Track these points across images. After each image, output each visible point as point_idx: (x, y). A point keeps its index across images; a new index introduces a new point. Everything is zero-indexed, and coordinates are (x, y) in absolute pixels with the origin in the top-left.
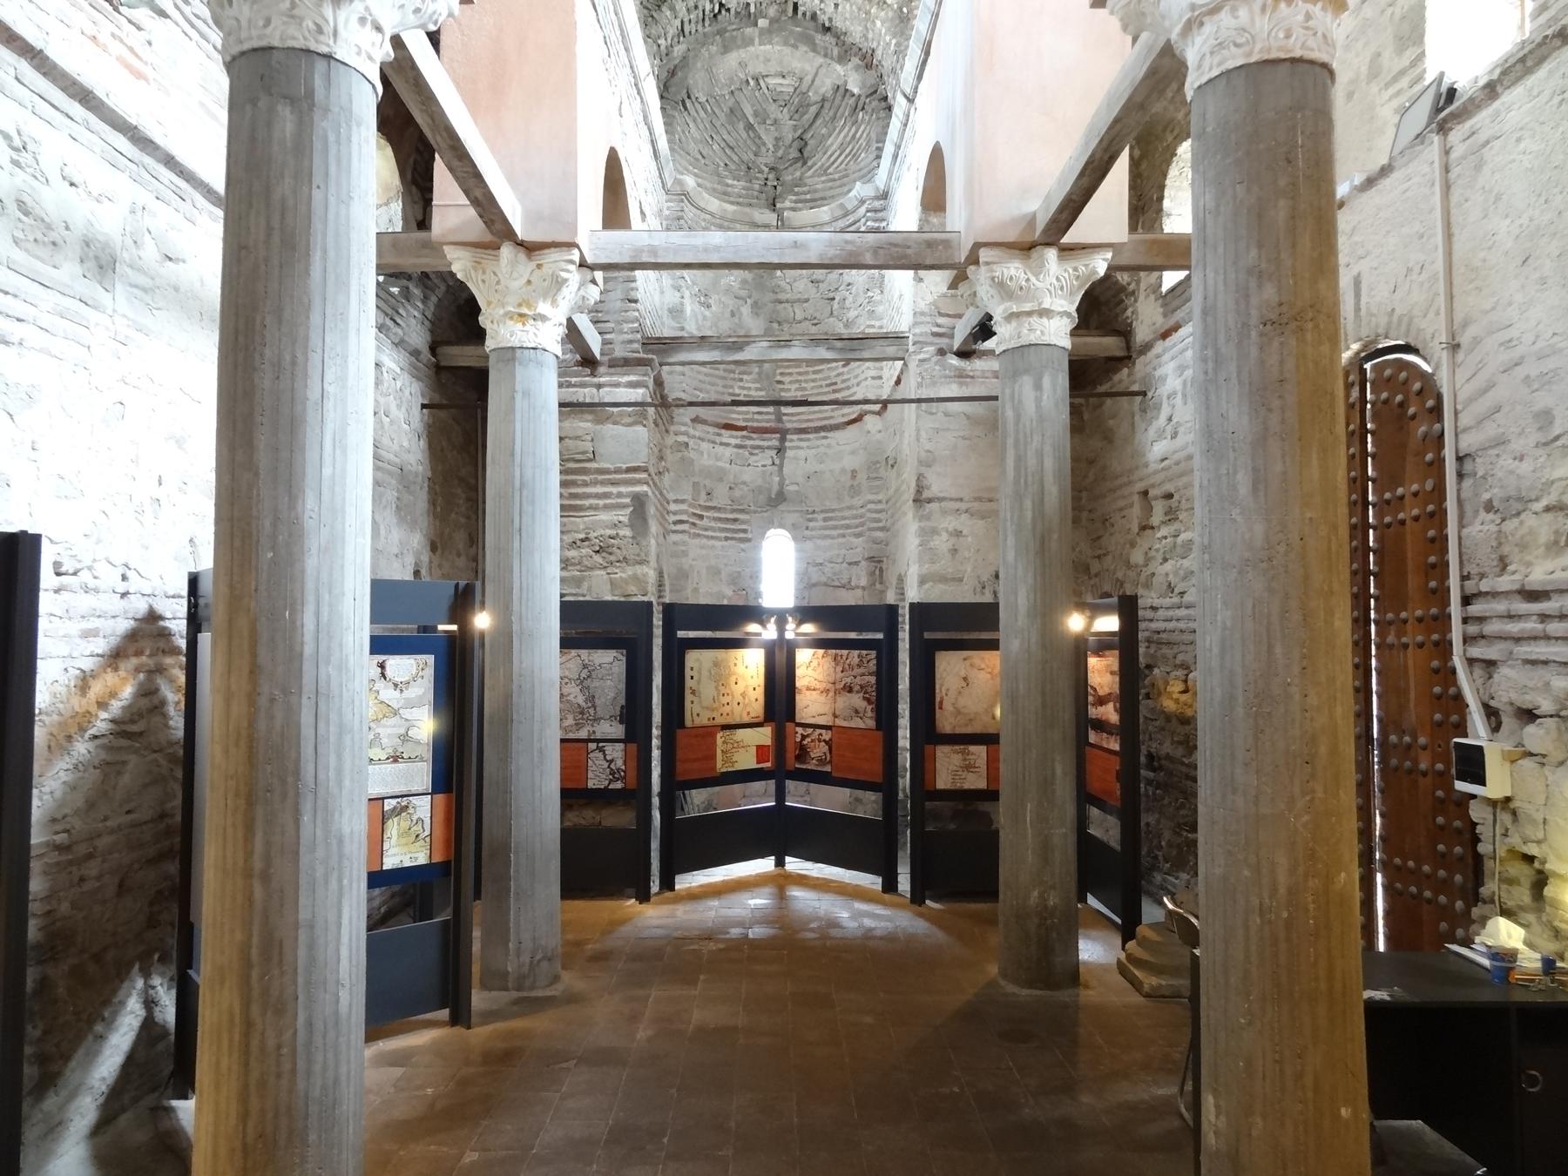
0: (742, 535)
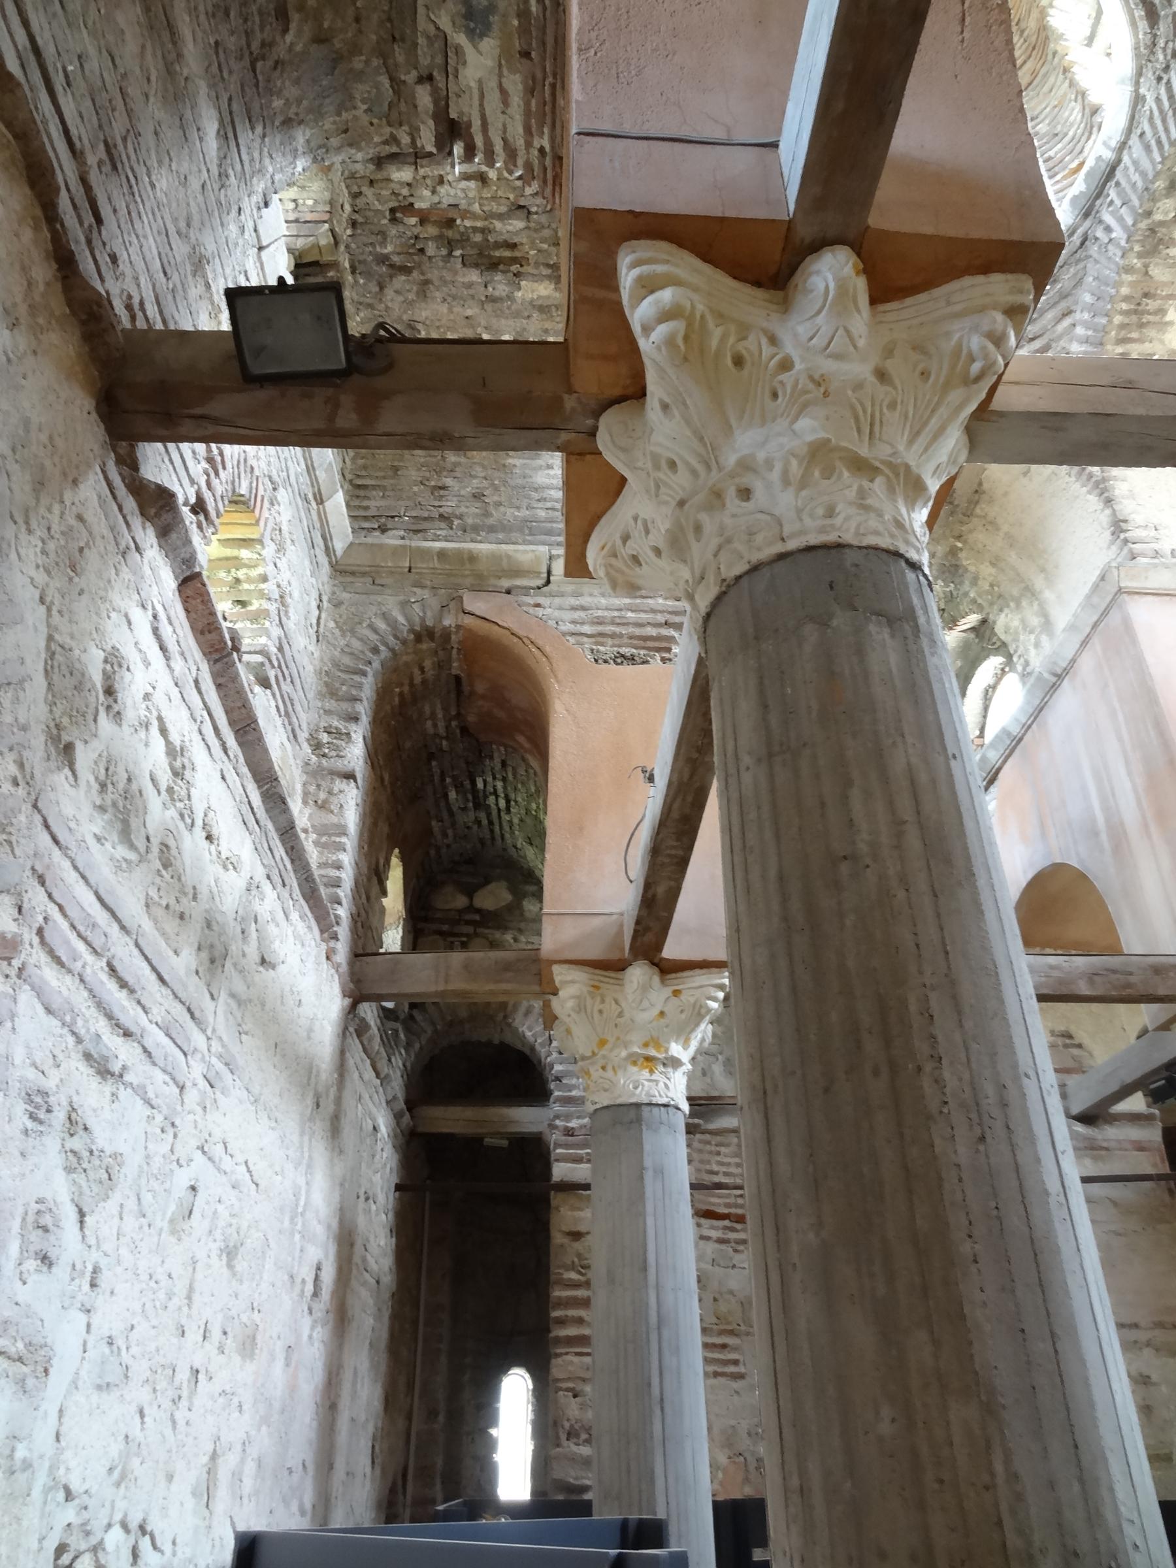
0: (732, 1369)
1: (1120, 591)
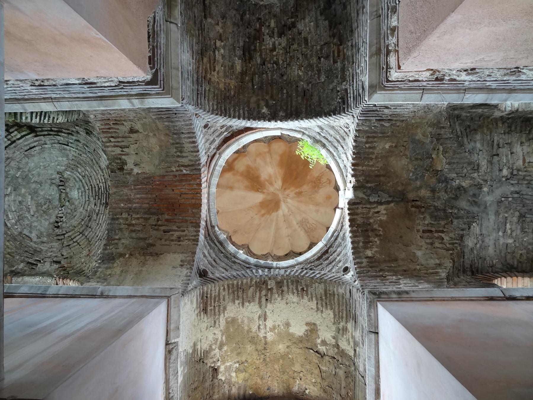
1: (168, 298)
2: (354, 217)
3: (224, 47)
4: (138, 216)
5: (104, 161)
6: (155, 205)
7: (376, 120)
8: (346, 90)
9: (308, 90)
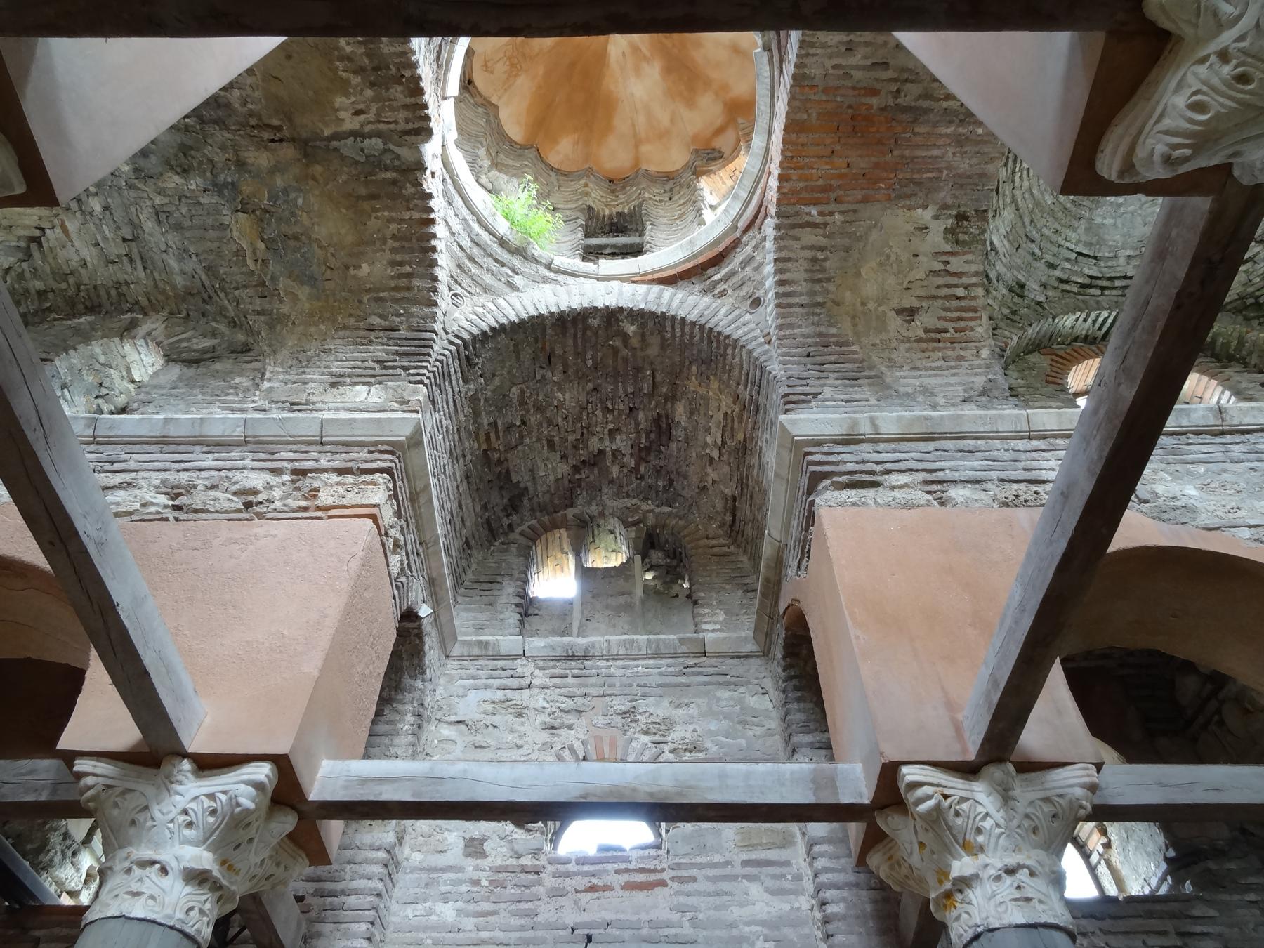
2: (412, 100)
3: (705, 445)
4: (945, 104)
5: (998, 233)
6: (899, 129)
7: (399, 330)
8: (466, 381)
9: (541, 367)
